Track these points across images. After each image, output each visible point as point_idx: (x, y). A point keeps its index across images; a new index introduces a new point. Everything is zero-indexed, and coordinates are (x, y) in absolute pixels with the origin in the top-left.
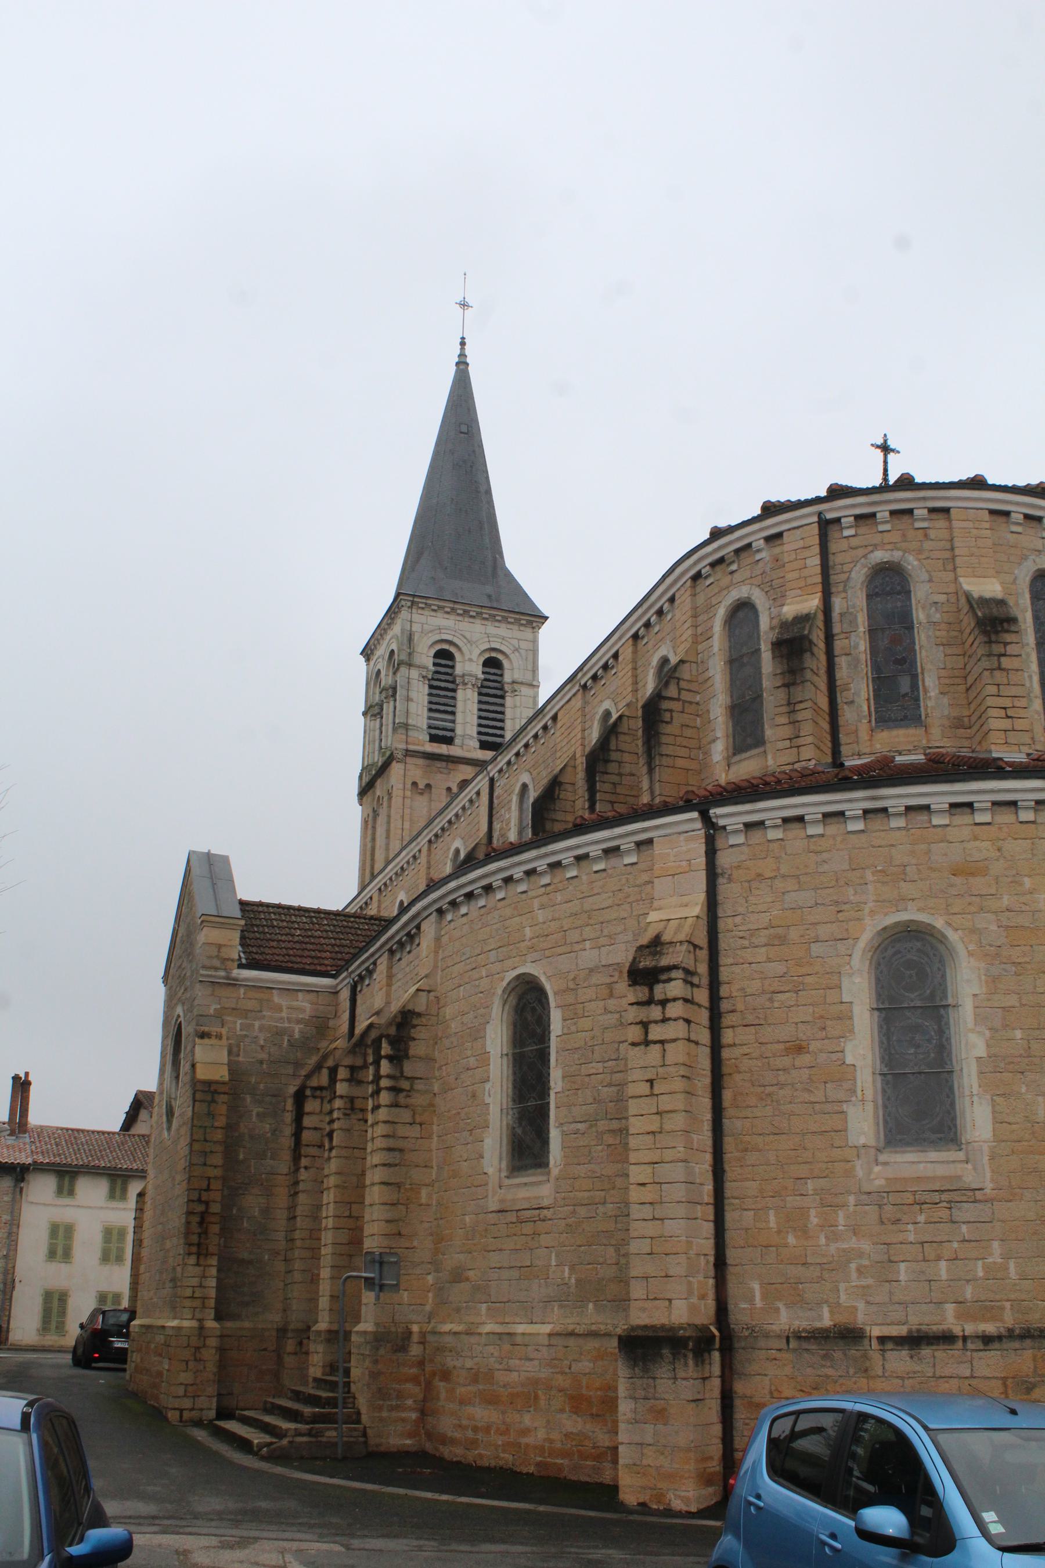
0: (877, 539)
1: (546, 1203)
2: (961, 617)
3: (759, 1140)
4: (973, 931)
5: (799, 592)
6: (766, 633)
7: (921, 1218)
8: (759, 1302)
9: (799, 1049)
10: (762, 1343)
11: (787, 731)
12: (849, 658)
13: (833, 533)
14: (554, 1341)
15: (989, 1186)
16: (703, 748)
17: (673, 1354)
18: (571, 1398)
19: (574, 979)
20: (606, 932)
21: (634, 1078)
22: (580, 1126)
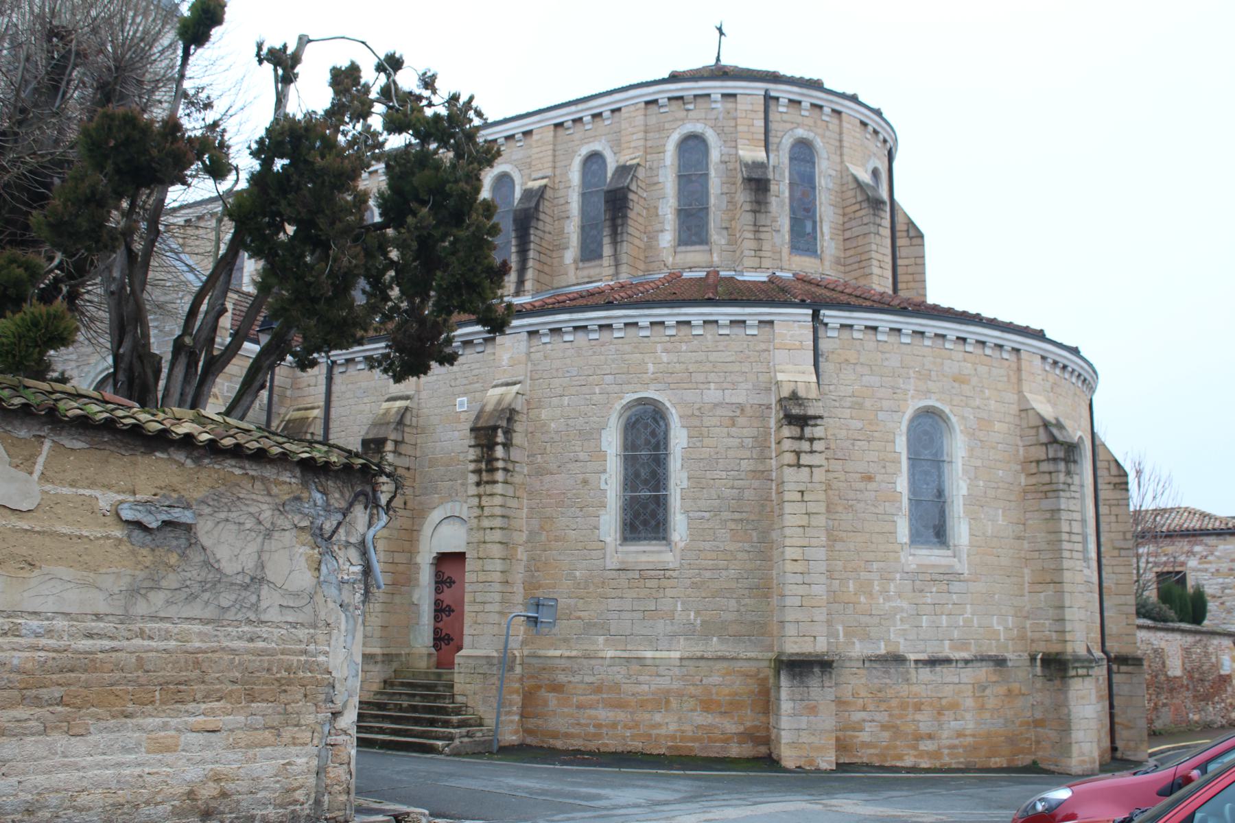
0: (799, 119)
1: (671, 566)
2: (844, 189)
3: (844, 534)
4: (963, 418)
5: (747, 142)
6: (716, 164)
7: (934, 589)
8: (842, 639)
9: (869, 478)
10: (848, 664)
11: (752, 244)
12: (778, 199)
13: (772, 103)
14: (684, 663)
15: (966, 572)
16: (652, 237)
17: (823, 672)
18: (701, 701)
19: (700, 409)
20: (729, 379)
21: (790, 488)
22: (704, 514)
